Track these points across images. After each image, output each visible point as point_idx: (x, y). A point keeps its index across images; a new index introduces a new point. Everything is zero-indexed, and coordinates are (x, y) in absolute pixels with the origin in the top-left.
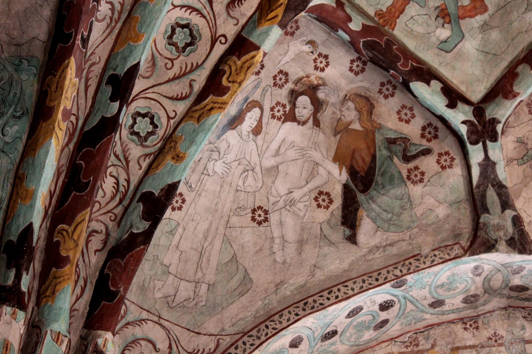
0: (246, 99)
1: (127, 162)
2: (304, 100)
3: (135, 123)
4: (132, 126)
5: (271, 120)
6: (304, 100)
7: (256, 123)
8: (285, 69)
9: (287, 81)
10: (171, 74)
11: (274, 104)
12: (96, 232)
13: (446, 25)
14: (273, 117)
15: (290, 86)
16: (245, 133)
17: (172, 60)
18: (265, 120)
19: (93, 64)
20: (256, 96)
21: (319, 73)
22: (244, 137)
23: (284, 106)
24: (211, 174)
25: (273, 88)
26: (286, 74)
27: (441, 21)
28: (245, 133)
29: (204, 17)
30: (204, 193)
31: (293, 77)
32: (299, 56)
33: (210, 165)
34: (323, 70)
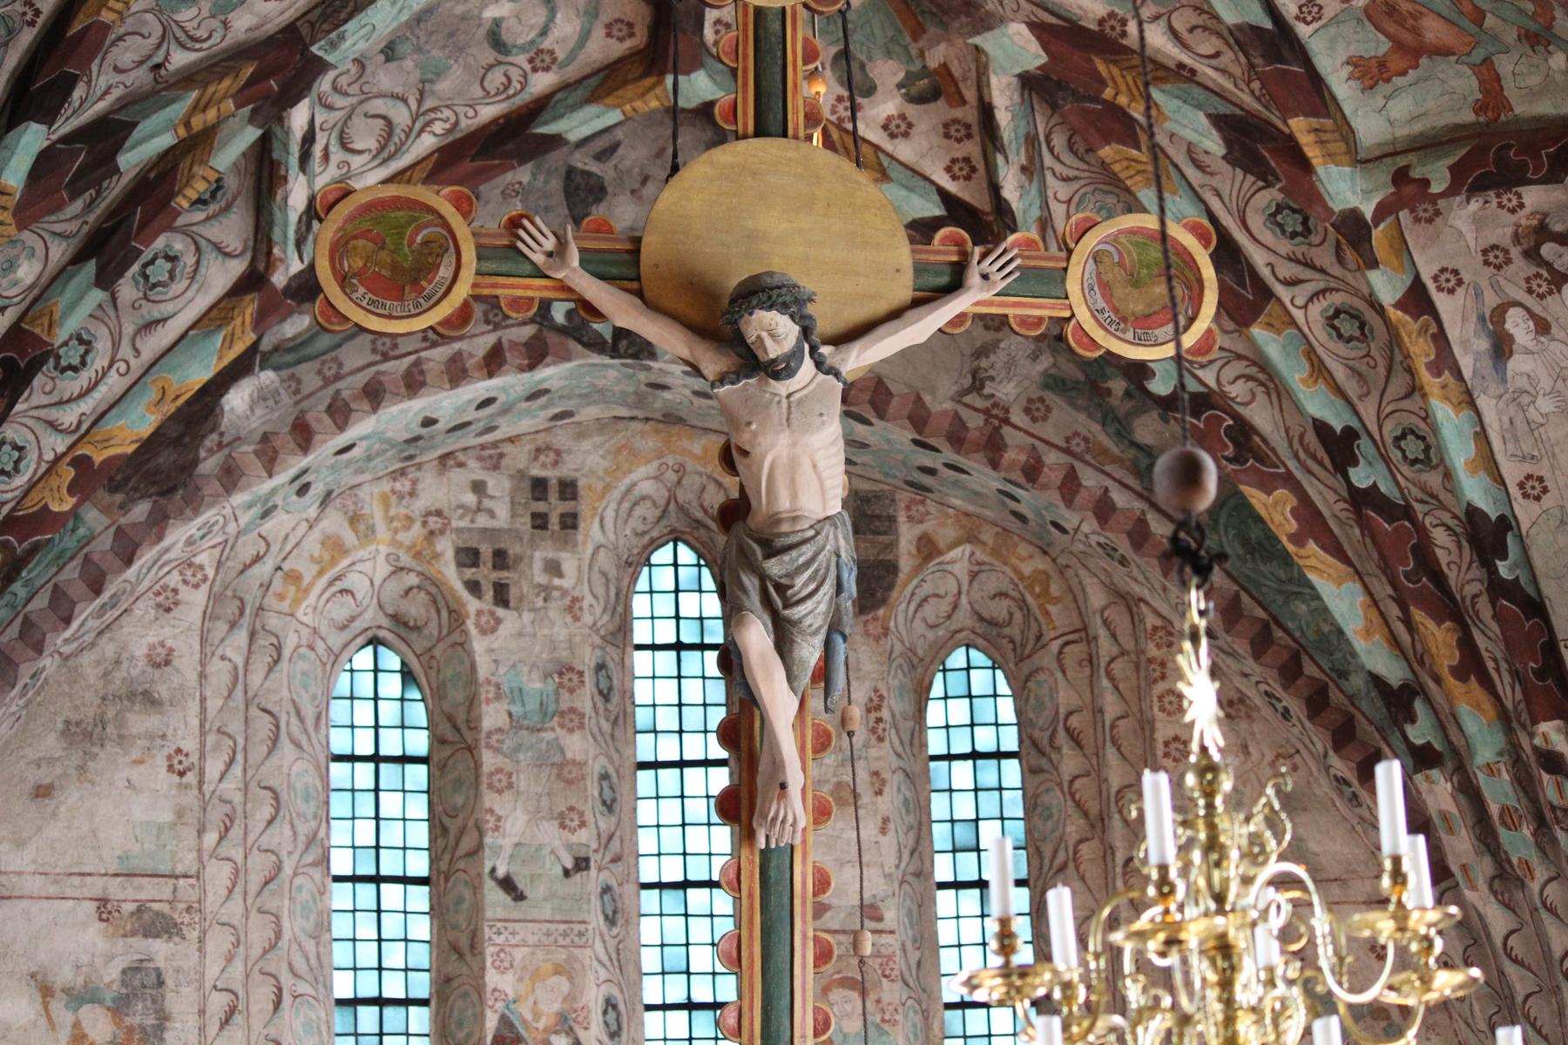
0: (1481, 319)
1: (1436, 498)
2: (1548, 250)
3: (1403, 452)
4: (1405, 457)
5: (1544, 302)
6: (1548, 250)
7: (1531, 323)
8: (1484, 244)
9: (1506, 252)
10: (1381, 370)
11: (1525, 286)
12: (1475, 596)
13: (1551, 48)
14: (1541, 297)
15: (1515, 252)
16: (1531, 345)
17: (1368, 355)
18: (1537, 310)
19: (1302, 437)
20: (1491, 300)
21: (1522, 213)
22: (1536, 349)
23: (1538, 276)
24: (1541, 420)
25: (1502, 272)
26: (1494, 247)
27: (1540, 48)
28: (1531, 345)
29: (1338, 290)
30: (1557, 450)
31: (1506, 241)
32: (1478, 222)
33: (1532, 413)
34: (1522, 206)
